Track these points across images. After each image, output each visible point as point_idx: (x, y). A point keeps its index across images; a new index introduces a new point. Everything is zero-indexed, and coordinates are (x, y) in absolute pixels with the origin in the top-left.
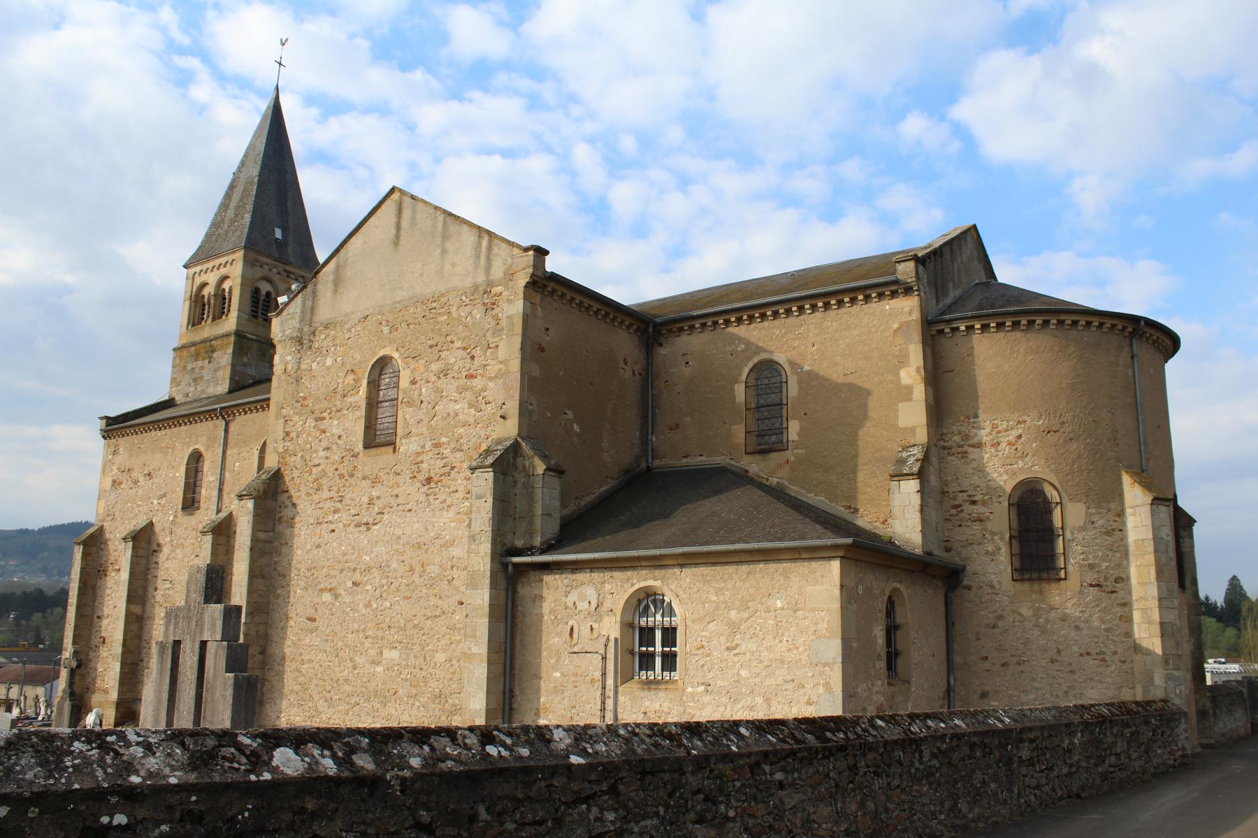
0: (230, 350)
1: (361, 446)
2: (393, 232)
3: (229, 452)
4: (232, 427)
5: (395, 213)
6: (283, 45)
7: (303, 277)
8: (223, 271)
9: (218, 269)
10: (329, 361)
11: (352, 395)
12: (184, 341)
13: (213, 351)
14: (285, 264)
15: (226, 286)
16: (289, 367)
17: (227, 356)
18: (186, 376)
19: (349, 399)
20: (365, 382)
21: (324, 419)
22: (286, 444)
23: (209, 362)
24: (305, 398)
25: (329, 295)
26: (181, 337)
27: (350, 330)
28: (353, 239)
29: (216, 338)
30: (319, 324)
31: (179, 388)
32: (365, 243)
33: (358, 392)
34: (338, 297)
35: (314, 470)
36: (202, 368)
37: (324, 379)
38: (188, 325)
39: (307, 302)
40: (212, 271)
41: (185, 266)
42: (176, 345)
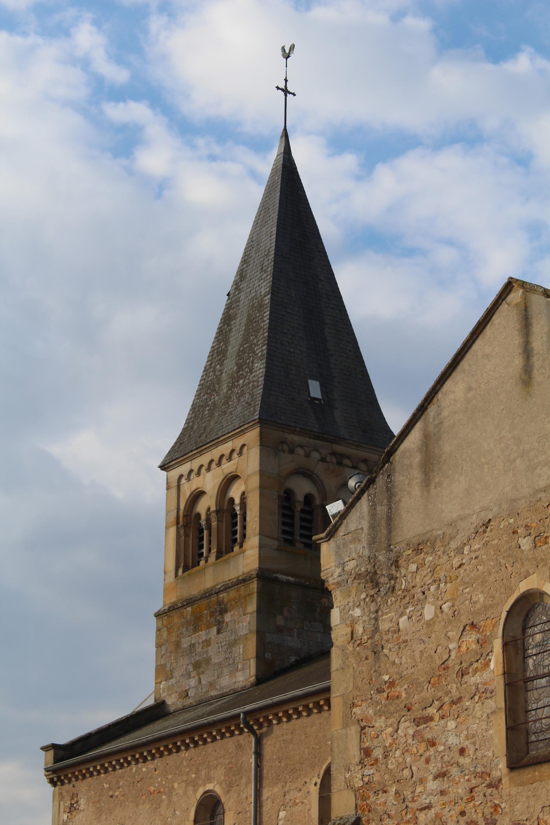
0: (252, 607)
1: (502, 764)
2: (518, 362)
3: (266, 793)
5: (518, 326)
7: (365, 461)
8: (228, 467)
9: (219, 464)
10: (429, 612)
11: (476, 671)
12: (172, 599)
13: (223, 611)
14: (332, 442)
15: (235, 493)
16: (359, 629)
17: (248, 618)
19: (472, 680)
20: (498, 644)
21: (431, 719)
22: (366, 772)
23: (219, 632)
24: (392, 684)
25: (416, 490)
26: (166, 591)
27: (459, 551)
28: (448, 385)
29: (227, 588)
30: (403, 545)
31: (173, 681)
32: (470, 389)
33: (487, 664)
34: (433, 492)
35: (422, 816)
36: (207, 642)
37: (422, 646)
39: (379, 508)
40: (209, 469)
41: (164, 467)
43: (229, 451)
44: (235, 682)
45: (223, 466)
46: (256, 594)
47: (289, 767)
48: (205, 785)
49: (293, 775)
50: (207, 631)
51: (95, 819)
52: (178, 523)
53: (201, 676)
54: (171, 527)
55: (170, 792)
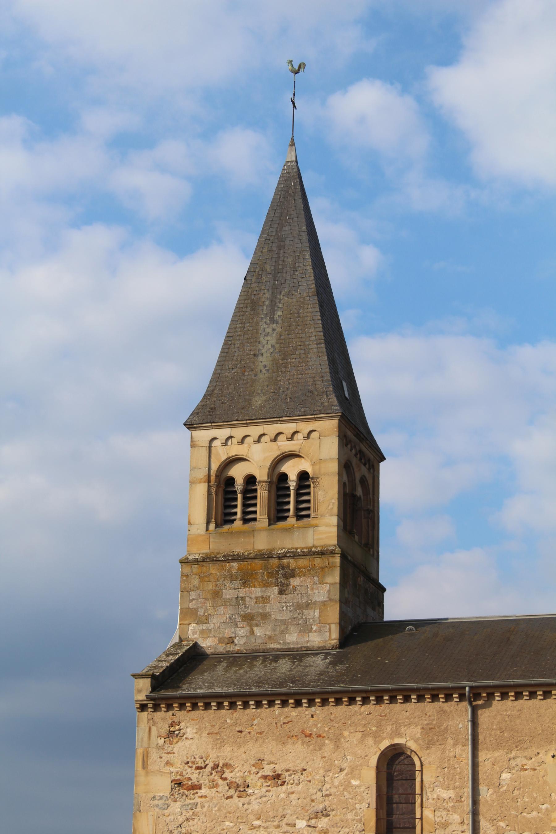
0: (335, 577)
3: (482, 756)
4: (484, 716)
6: (296, 72)
8: (285, 445)
9: (275, 439)
18: (221, 610)
23: (281, 592)
26: (191, 541)
29: (295, 555)
31: (205, 627)
38: (208, 523)
40: (258, 441)
41: (190, 425)
42: (183, 555)
43: (292, 431)
44: (308, 641)
45: (279, 443)
46: (338, 569)
47: (515, 738)
48: (392, 738)
49: (522, 745)
50: (264, 589)
51: (213, 749)
52: (209, 482)
53: (255, 629)
54: (200, 483)
55: (337, 740)
